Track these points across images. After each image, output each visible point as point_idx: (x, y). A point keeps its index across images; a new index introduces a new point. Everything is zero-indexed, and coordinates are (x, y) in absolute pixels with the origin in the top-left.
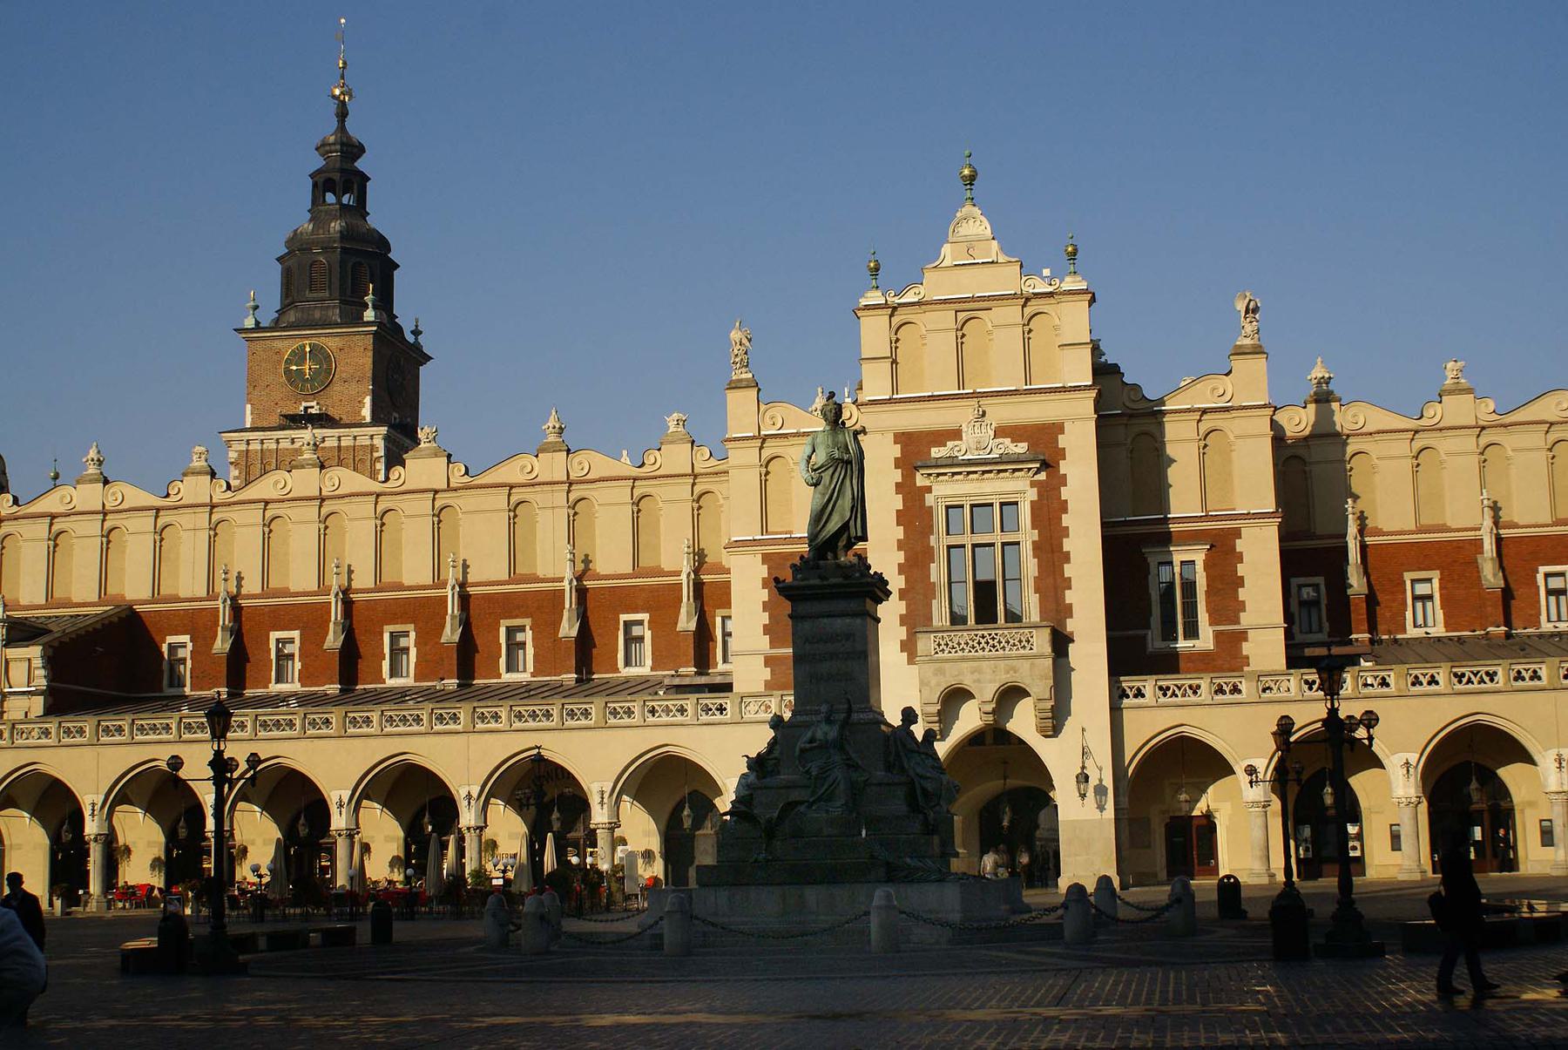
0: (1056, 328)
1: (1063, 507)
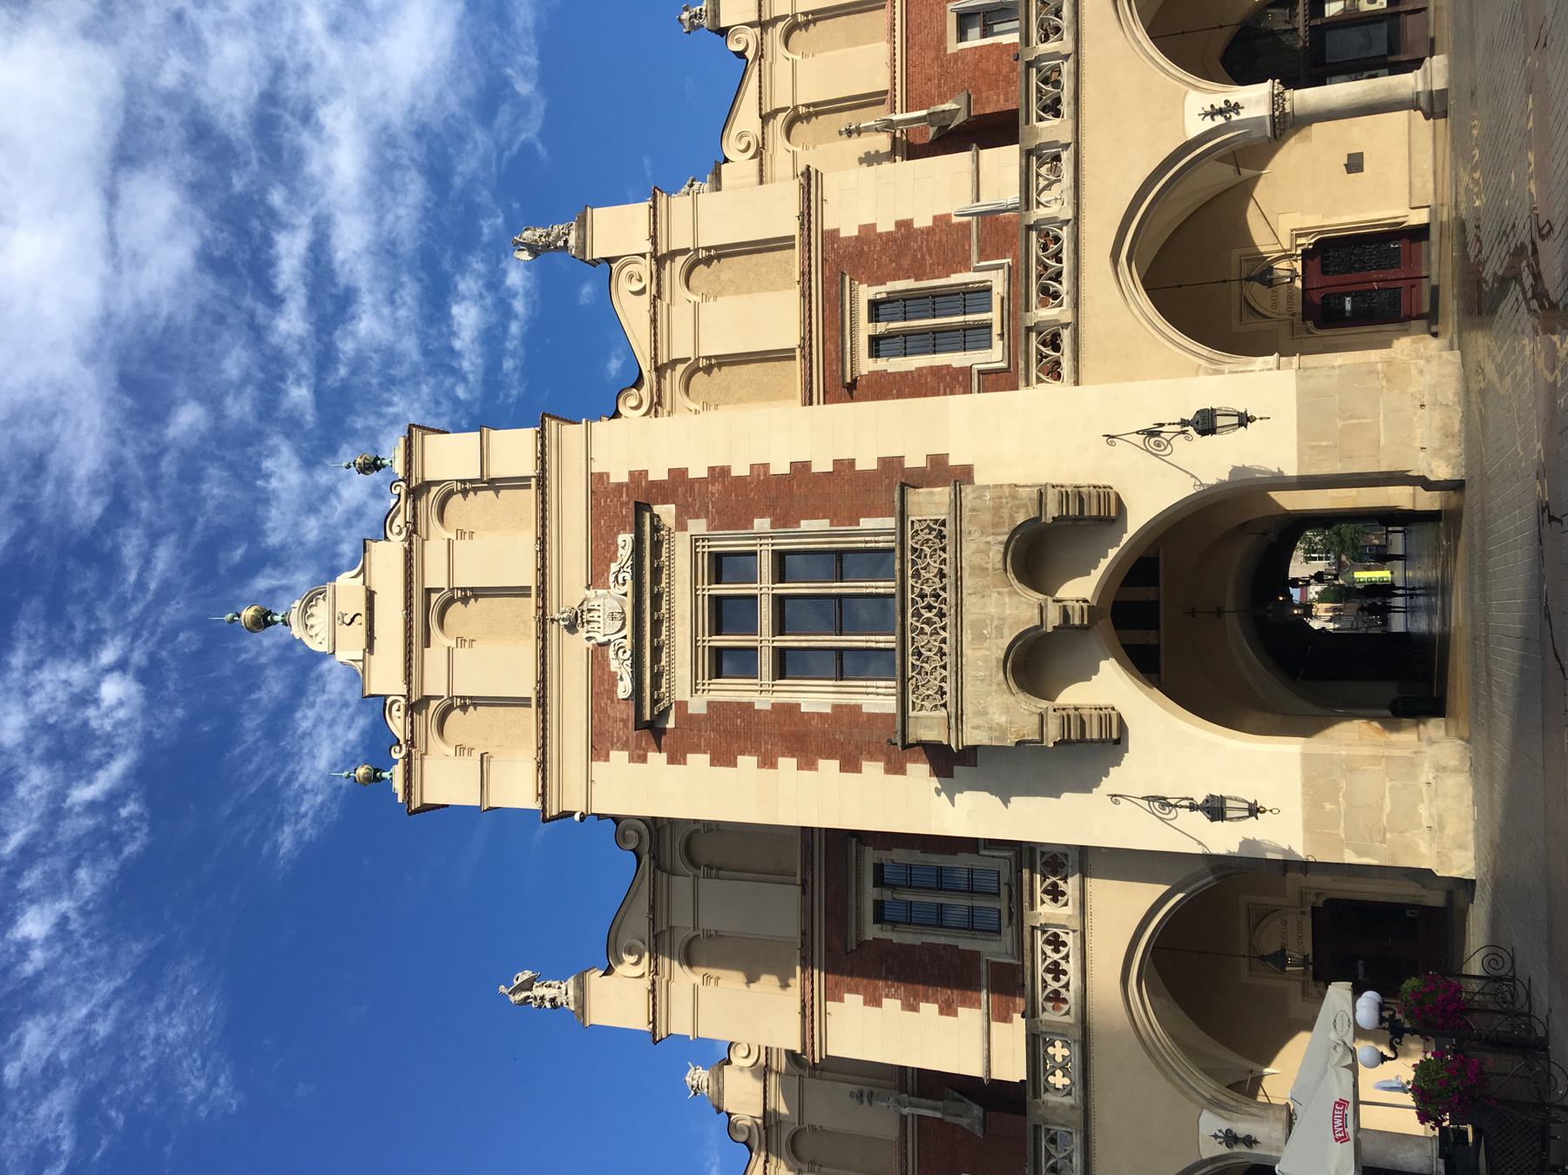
1: (719, 474)
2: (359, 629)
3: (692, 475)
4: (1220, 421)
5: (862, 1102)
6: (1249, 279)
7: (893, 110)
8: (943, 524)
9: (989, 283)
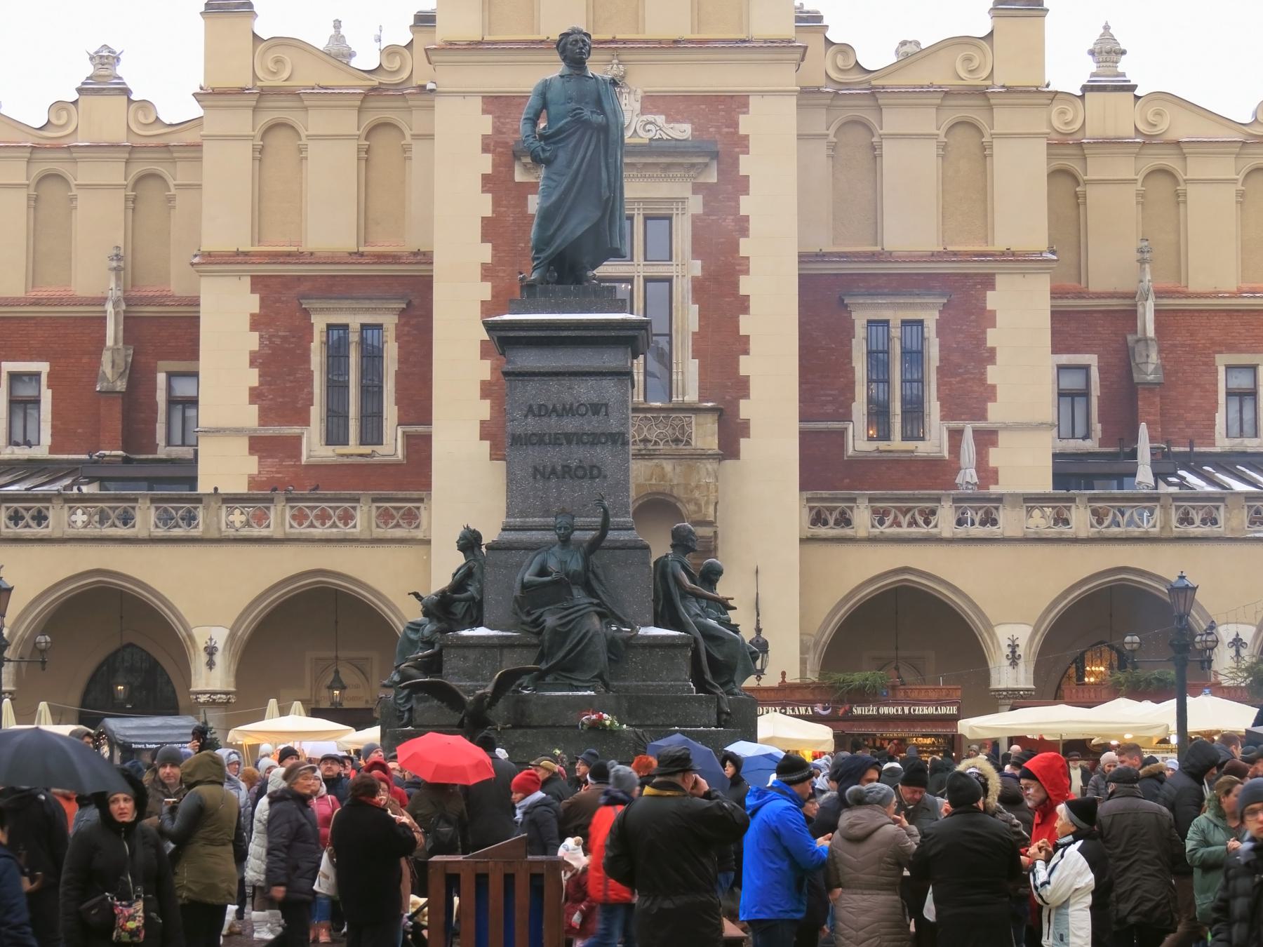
3: (743, 199)
5: (112, 260)
8: (688, 443)
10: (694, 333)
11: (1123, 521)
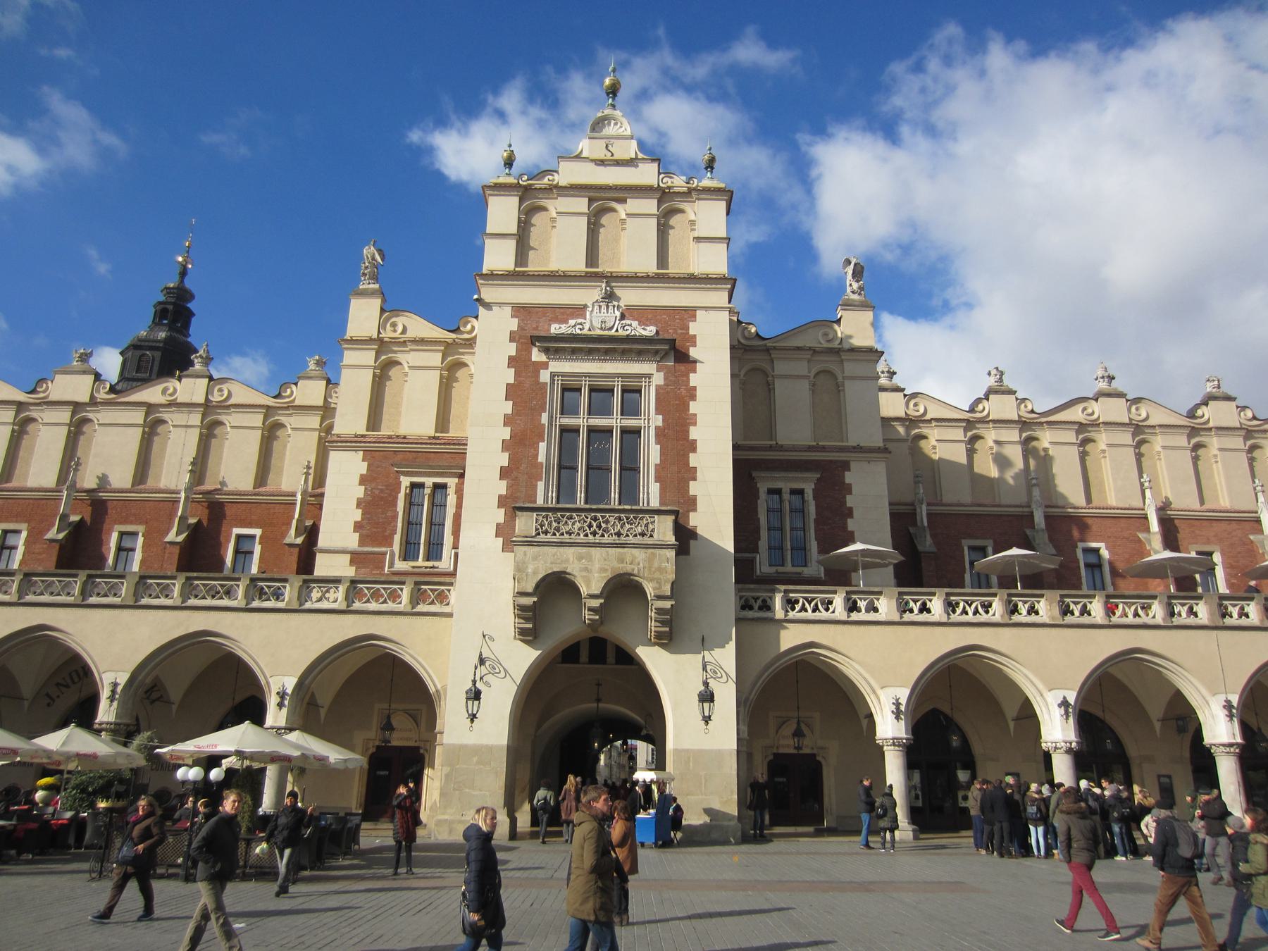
0: (692, 223)
2: (602, 154)
3: (691, 375)
4: (706, 705)
6: (798, 723)
7: (928, 504)
8: (651, 536)
9: (809, 565)
10: (656, 465)
11: (970, 611)
